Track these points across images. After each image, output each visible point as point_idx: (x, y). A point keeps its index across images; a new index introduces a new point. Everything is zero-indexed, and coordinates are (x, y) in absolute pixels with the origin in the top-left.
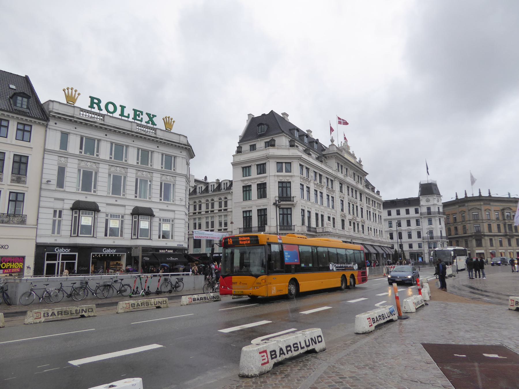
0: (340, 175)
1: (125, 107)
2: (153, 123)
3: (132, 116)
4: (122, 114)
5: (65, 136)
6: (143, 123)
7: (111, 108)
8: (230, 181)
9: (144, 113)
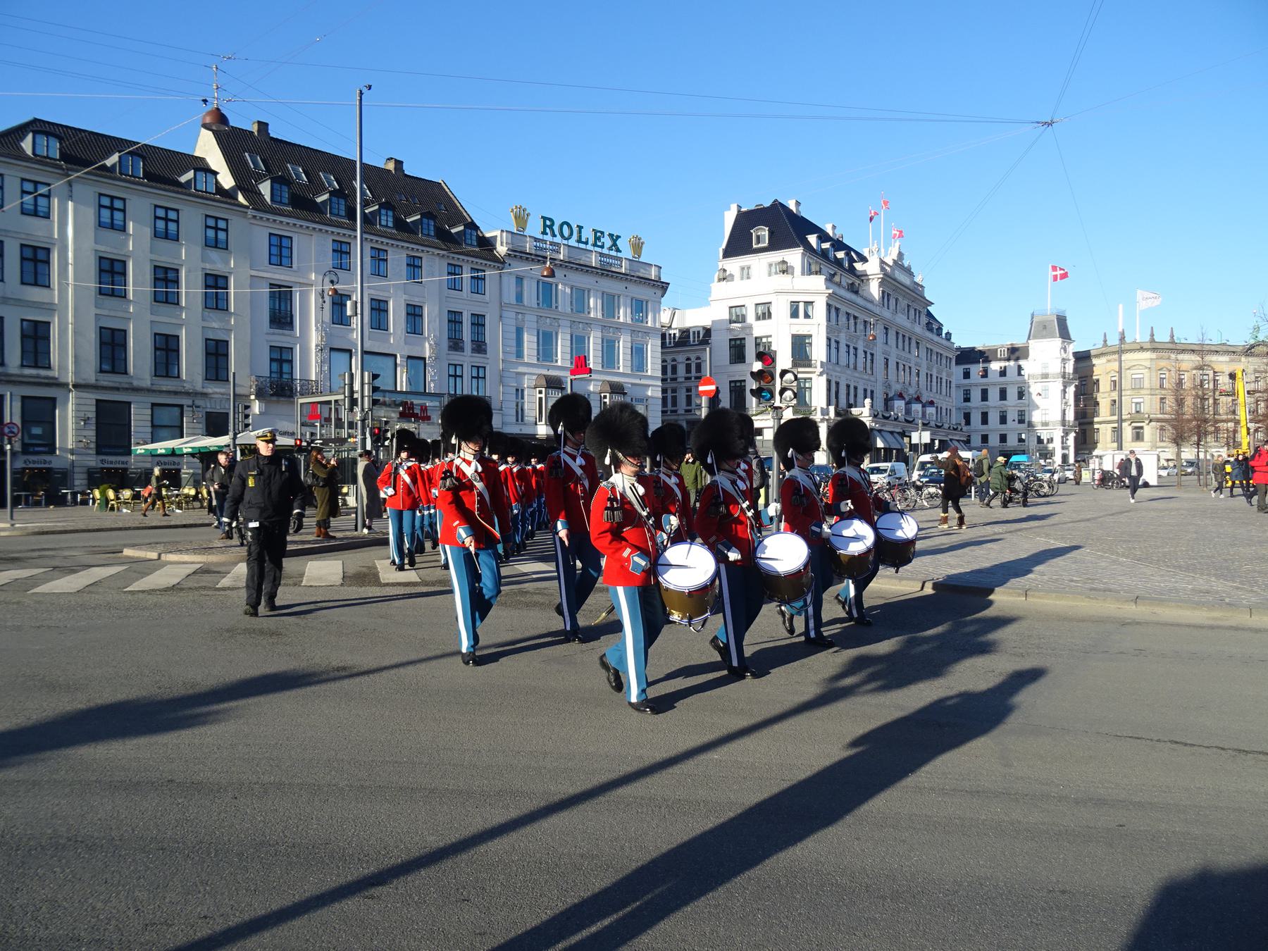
0: (887, 314)
2: (618, 250)
3: (591, 241)
4: (579, 241)
5: (520, 280)
6: (605, 251)
7: (566, 231)
8: (704, 328)
9: (606, 234)
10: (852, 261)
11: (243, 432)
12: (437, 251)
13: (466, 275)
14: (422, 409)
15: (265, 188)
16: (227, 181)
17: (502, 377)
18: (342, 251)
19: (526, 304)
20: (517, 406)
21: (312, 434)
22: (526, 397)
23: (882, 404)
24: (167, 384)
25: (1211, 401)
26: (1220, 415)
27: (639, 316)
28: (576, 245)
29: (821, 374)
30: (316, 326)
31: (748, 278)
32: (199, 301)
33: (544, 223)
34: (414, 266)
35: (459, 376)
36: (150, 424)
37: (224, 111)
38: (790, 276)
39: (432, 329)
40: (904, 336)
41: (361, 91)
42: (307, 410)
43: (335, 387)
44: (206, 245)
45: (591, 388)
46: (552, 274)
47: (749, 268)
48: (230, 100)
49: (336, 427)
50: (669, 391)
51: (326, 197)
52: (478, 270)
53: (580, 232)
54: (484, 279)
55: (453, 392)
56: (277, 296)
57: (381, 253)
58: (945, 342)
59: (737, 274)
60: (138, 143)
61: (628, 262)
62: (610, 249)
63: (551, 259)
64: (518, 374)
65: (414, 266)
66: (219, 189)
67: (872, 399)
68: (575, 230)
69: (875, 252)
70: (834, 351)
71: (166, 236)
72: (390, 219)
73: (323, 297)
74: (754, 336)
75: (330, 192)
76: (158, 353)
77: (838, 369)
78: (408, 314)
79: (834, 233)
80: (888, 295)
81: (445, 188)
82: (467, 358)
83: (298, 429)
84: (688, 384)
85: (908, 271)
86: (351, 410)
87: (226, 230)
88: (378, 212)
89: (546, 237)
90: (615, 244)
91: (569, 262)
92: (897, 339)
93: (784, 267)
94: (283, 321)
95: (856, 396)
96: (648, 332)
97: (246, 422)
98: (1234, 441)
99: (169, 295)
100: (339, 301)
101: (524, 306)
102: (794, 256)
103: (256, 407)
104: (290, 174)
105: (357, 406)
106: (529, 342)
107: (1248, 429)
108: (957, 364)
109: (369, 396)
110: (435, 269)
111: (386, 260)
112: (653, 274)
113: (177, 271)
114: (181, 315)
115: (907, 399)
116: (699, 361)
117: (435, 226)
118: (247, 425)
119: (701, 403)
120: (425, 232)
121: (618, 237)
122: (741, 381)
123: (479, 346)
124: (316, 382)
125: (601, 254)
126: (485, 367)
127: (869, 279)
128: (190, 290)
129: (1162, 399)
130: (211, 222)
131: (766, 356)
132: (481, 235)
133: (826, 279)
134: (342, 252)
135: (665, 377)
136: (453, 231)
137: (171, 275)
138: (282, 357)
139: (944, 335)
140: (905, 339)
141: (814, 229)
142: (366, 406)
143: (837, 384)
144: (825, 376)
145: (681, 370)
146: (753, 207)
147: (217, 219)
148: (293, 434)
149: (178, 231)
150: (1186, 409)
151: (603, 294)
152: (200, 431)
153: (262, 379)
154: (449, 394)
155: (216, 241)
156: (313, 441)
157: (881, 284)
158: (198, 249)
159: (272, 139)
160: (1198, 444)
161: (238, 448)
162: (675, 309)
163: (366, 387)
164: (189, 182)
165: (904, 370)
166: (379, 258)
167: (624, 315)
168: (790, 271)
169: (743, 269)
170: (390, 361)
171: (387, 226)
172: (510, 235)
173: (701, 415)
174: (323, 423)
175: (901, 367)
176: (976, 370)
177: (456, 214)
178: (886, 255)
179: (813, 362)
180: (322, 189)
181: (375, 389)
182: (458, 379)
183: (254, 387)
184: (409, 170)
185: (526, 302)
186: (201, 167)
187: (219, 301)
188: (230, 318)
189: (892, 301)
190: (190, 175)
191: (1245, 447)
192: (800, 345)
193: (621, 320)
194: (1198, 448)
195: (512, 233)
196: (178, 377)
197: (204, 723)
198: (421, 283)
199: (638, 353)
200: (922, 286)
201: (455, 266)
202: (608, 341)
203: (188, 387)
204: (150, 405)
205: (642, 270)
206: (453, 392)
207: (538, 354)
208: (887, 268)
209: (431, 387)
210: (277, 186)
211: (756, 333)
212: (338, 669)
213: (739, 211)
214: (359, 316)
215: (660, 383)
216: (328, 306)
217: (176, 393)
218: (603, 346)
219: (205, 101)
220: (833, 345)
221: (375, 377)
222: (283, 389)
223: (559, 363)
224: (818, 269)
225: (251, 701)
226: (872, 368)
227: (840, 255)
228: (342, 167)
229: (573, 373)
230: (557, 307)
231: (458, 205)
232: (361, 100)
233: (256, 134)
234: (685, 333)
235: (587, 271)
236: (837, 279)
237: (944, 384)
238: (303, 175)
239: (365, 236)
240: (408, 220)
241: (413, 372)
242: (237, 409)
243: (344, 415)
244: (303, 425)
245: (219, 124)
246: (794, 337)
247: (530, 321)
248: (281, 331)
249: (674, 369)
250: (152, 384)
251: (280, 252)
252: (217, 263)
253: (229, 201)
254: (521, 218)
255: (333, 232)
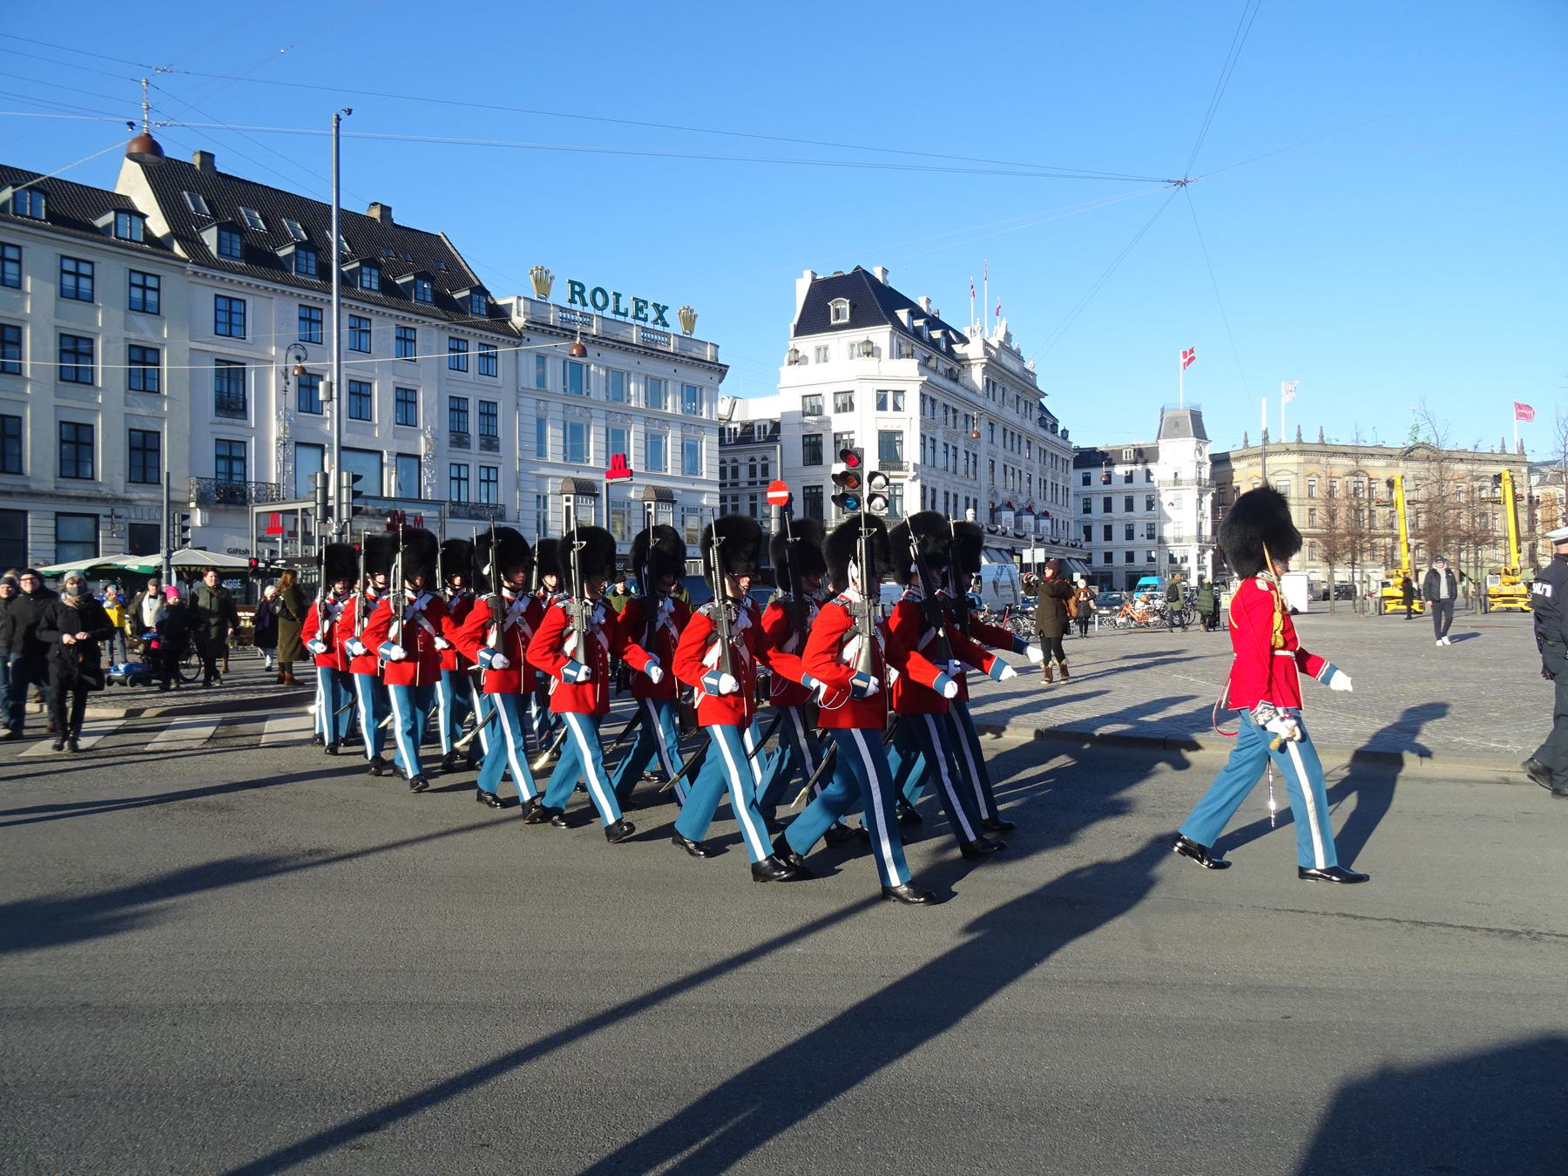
1: (620, 295)
2: (665, 324)
3: (631, 312)
4: (617, 312)
5: (541, 358)
6: (649, 325)
8: (771, 421)
10: (950, 342)
11: (180, 549)
12: (435, 322)
13: (473, 352)
14: (416, 520)
15: (210, 237)
16: (159, 226)
17: (518, 480)
18: (311, 319)
19: (549, 389)
20: (538, 517)
21: (272, 552)
22: (549, 506)
23: (988, 515)
24: (76, 488)
25: (1366, 513)
26: (1376, 529)
27: (691, 406)
28: (612, 316)
29: (914, 479)
30: (277, 414)
31: (826, 361)
32: (121, 381)
33: (573, 288)
34: (406, 340)
35: (464, 479)
36: (52, 539)
37: (156, 138)
38: (876, 359)
39: (428, 419)
40: (1012, 434)
41: (338, 116)
42: (267, 521)
43: (302, 492)
44: (130, 309)
45: (632, 495)
46: (583, 353)
47: (826, 349)
48: (164, 125)
49: (305, 542)
50: (729, 499)
51: (290, 250)
52: (488, 346)
53: (617, 301)
54: (496, 357)
55: (456, 499)
56: (226, 375)
57: (363, 323)
58: (1060, 441)
59: (812, 356)
60: (39, 175)
61: (677, 339)
62: (655, 322)
63: (581, 333)
64: (539, 476)
65: (406, 340)
66: (149, 237)
67: (975, 509)
68: (612, 298)
69: (978, 332)
70: (929, 451)
71: (77, 296)
72: (375, 280)
73: (286, 378)
74: (834, 431)
75: (297, 244)
76: (65, 447)
77: (934, 472)
78: (398, 400)
79: (928, 308)
80: (994, 384)
81: (446, 242)
82: (474, 456)
83: (253, 546)
84: (753, 490)
85: (1017, 356)
86: (325, 520)
87: (158, 290)
88: (359, 270)
89: (574, 307)
90: (661, 317)
91: (604, 338)
92: (1005, 437)
93: (869, 348)
94: (233, 407)
95: (956, 505)
96: (702, 426)
97: (184, 536)
98: (1393, 560)
99: (81, 372)
100: (308, 383)
101: (547, 391)
102: (881, 335)
103: (197, 518)
104: (243, 220)
105: (332, 516)
106: (554, 437)
107: (1409, 545)
108: (1076, 466)
109: (348, 503)
110: (432, 343)
111: (370, 332)
112: (708, 354)
113: (91, 341)
114: (96, 398)
115: (1017, 510)
116: (765, 462)
117: (432, 290)
118: (185, 541)
119: (770, 514)
120: (420, 297)
121: (665, 308)
122: (817, 487)
123: (489, 442)
124: (277, 485)
125: (644, 329)
126: (497, 468)
127: (970, 365)
128: (108, 365)
129: (1311, 510)
130: (137, 279)
131: (850, 455)
132: (492, 302)
133: (919, 364)
134: (311, 320)
135: (724, 481)
136: (456, 296)
137: (83, 347)
138: (231, 454)
139: (1059, 433)
140: (1013, 436)
141: (905, 303)
142: (344, 515)
143: (934, 491)
144: (919, 481)
145: (744, 473)
146: (830, 275)
147: (145, 275)
148: (246, 552)
149: (93, 290)
150: (1338, 522)
151: (646, 378)
152: (120, 549)
153: (204, 482)
154: (451, 501)
155: (144, 303)
156: (273, 562)
157: (985, 371)
158: (119, 314)
159: (220, 174)
160: (1353, 564)
161: (173, 570)
162: (735, 398)
163: (344, 491)
164: (107, 227)
165: (1013, 475)
166: (359, 331)
167: (672, 405)
168: (876, 353)
169: (819, 349)
170: (376, 458)
171: (370, 289)
172: (529, 303)
173: (770, 528)
174: (286, 537)
175: (1009, 471)
176: (1097, 474)
177: (459, 275)
178: (991, 335)
179: (904, 464)
180: (284, 240)
181: (356, 494)
182: (462, 482)
183: (194, 491)
184: (398, 218)
185: (549, 385)
186: (125, 207)
187: (148, 380)
188: (163, 402)
189: (999, 392)
190: (109, 217)
191: (1405, 566)
192: (889, 443)
193: (669, 410)
194: (1353, 568)
195: (532, 300)
196: (92, 478)
197: (131, 928)
198: (415, 361)
199: (690, 452)
200: (1033, 374)
201: (458, 340)
202: (653, 437)
203: (105, 491)
204: (53, 515)
205: (695, 350)
206: (456, 499)
207: (565, 452)
208: (992, 351)
209: (428, 493)
210: (225, 234)
211: (835, 429)
212: (310, 853)
213: (814, 279)
214: (335, 401)
215: (717, 489)
216: (293, 388)
217: (89, 499)
218: (646, 443)
219: (131, 124)
220: (929, 444)
221: (356, 478)
222: (233, 494)
223: (592, 464)
224: (910, 352)
225: (195, 897)
226: (975, 472)
227: (937, 334)
228: (313, 213)
229: (609, 475)
230: (588, 394)
231: (463, 264)
232: (338, 127)
233: (198, 167)
234: (748, 427)
235: (627, 349)
236: (932, 363)
237: (1060, 491)
238: (260, 221)
239: (343, 301)
240: (397, 282)
241: (404, 473)
242: (171, 521)
243: (314, 528)
244: (259, 540)
245: (150, 156)
246: (881, 433)
247: (555, 410)
248: (230, 420)
249: (735, 472)
250: (56, 488)
251: (230, 319)
252: (145, 331)
253: (161, 252)
254: (543, 282)
255: (299, 295)
